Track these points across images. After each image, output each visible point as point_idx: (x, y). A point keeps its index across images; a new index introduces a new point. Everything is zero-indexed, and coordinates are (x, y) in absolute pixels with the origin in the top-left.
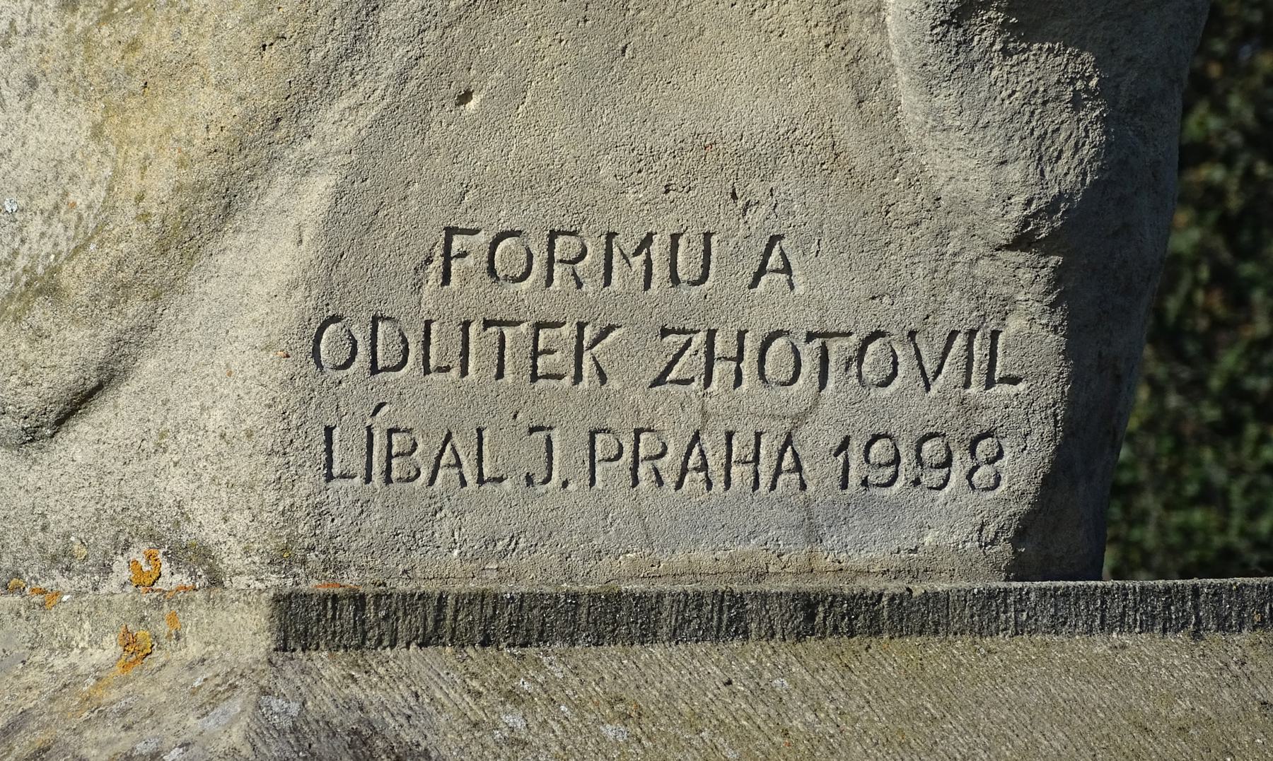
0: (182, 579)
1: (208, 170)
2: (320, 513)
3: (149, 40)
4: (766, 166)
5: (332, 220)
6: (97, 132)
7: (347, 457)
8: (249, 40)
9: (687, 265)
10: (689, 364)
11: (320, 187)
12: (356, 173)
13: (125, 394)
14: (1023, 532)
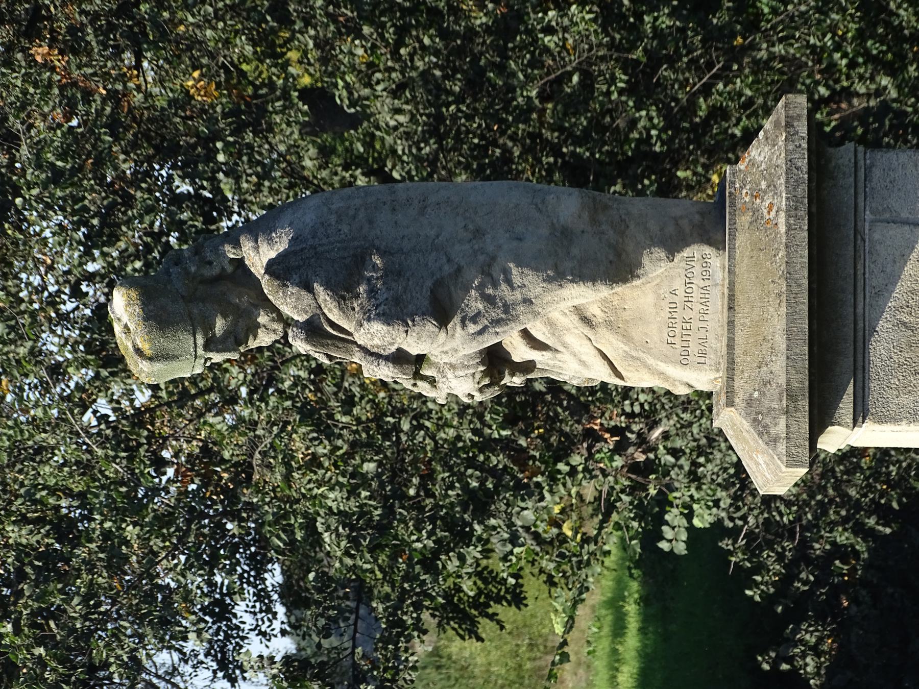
1: (656, 377)
2: (711, 365)
4: (659, 295)
5: (665, 362)
7: (702, 360)
9: (674, 306)
10: (689, 304)
11: (659, 363)
12: (658, 359)
14: (718, 249)
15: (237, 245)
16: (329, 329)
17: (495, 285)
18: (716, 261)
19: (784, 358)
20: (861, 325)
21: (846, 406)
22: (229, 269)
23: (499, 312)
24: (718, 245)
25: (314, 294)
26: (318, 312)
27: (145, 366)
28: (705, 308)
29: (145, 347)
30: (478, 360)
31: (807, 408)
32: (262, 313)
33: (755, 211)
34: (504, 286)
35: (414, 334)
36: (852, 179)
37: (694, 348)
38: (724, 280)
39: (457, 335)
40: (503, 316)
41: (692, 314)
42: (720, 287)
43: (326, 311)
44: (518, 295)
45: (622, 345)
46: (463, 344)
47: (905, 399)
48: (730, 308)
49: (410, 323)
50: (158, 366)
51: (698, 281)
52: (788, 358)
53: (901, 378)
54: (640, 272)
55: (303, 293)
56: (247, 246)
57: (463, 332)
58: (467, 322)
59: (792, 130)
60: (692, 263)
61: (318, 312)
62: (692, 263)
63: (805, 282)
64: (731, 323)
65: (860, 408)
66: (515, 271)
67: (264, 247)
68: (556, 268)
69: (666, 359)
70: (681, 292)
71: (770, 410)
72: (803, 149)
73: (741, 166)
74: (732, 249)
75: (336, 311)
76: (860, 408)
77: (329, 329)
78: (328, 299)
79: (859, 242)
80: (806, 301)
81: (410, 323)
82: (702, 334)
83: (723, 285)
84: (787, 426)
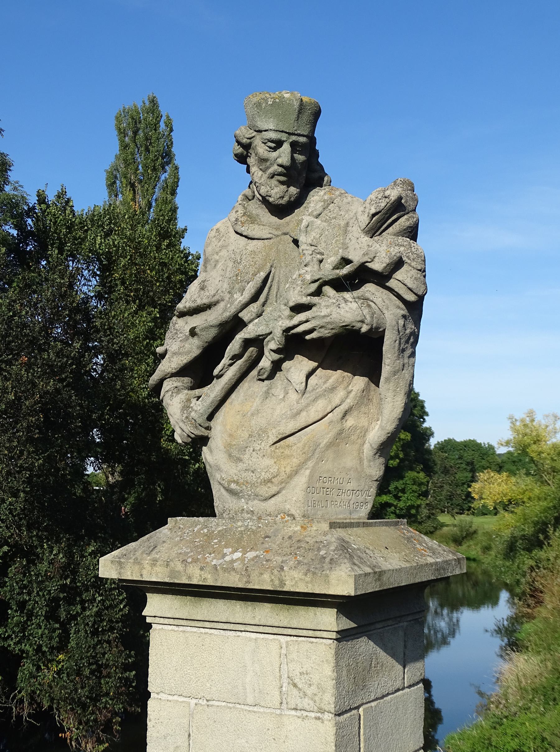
0: (289, 518)
1: (295, 469)
3: (286, 452)
6: (275, 463)
8: (301, 453)
10: (341, 493)
11: (308, 472)
12: (312, 470)
13: (280, 495)
18: (364, 511)
21: (347, 624)
26: (407, 211)
31: (376, 590)
32: (298, 190)
35: (419, 275)
38: (353, 519)
39: (398, 311)
42: (349, 517)
43: (406, 217)
45: (324, 443)
46: (393, 314)
47: (345, 673)
51: (354, 499)
52: (393, 570)
54: (377, 456)
69: (311, 476)
70: (350, 486)
74: (370, 525)
75: (408, 224)
79: (399, 619)
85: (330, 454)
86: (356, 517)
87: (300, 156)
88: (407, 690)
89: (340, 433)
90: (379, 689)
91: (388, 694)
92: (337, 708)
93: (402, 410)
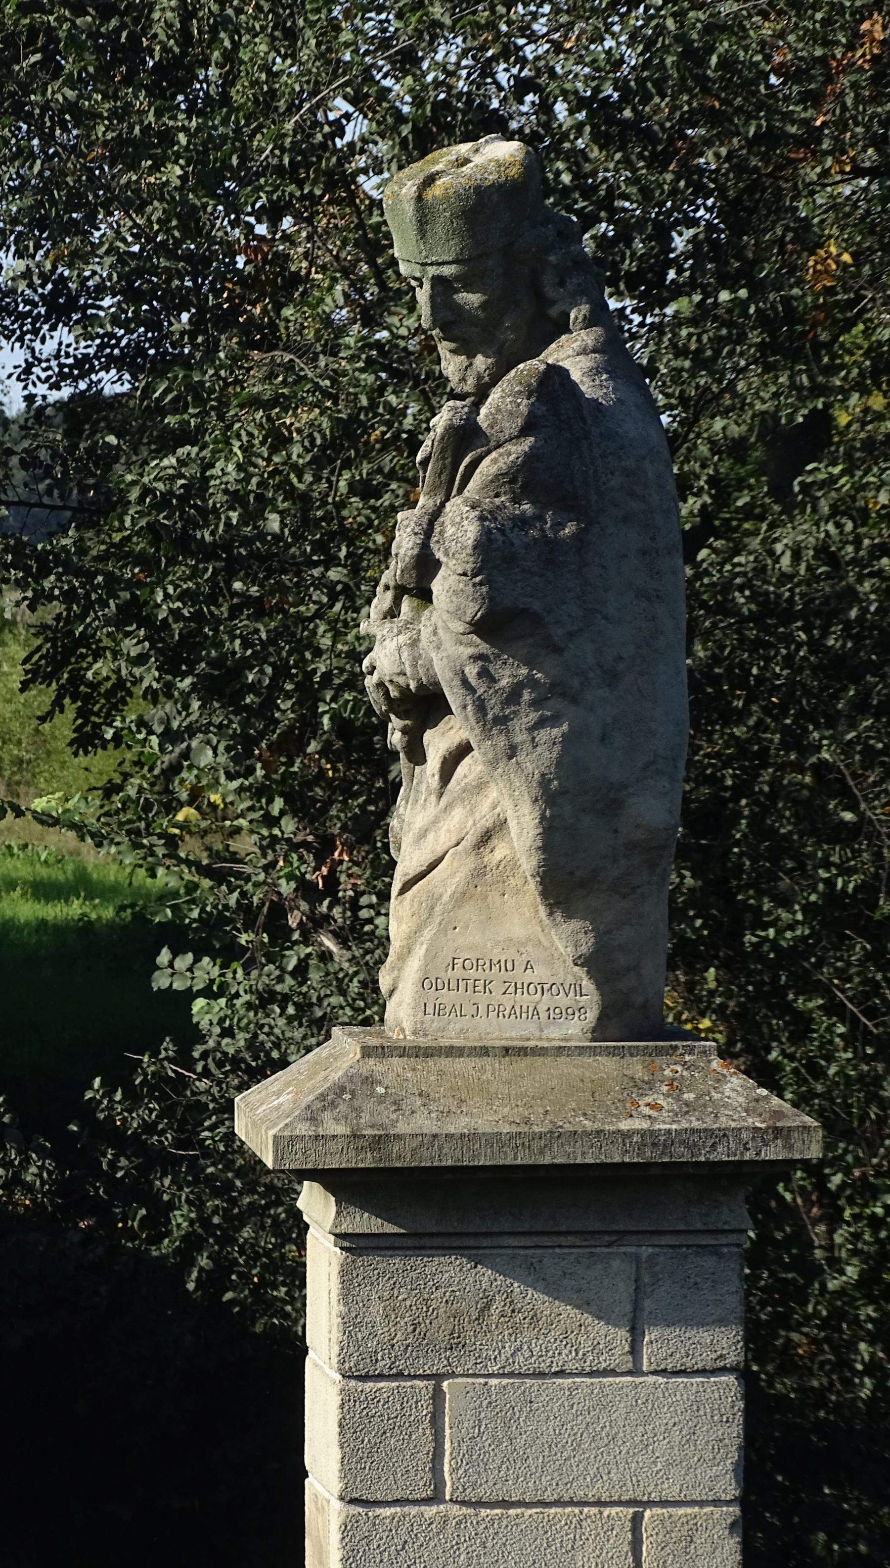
2: (422, 1023)
4: (524, 944)
5: (426, 956)
7: (430, 1010)
9: (509, 967)
10: (512, 989)
11: (425, 947)
14: (594, 1031)
15: (589, 323)
16: (467, 460)
17: (535, 704)
19: (435, 1130)
20: (486, 1242)
22: (554, 312)
23: (497, 710)
24: (600, 1031)
25: (517, 437)
26: (492, 444)
27: (409, 189)
28: (507, 1013)
29: (437, 190)
30: (424, 680)
33: (650, 1085)
34: (534, 716)
36: (699, 1226)
37: (446, 997)
39: (461, 649)
40: (490, 716)
41: (497, 995)
42: (537, 1034)
43: (494, 455)
44: (521, 737)
46: (448, 657)
47: (376, 1310)
48: (507, 1050)
49: (478, 579)
50: (409, 209)
52: (435, 1136)
53: (408, 1303)
54: (558, 916)
55: (520, 421)
56: (586, 337)
57: (465, 657)
58: (480, 663)
59: (771, 1137)
60: (572, 994)
61: (492, 444)
62: (572, 994)
63: (547, 1160)
64: (484, 1051)
65: (362, 1243)
66: (556, 732)
67: (586, 362)
68: (562, 792)
69: (430, 957)
70: (529, 977)
71: (358, 1111)
72: (742, 1154)
73: (716, 1063)
74: (594, 1052)
75: (494, 470)
76: (362, 1243)
77: (467, 460)
78: (512, 458)
79: (607, 1238)
80: (519, 1162)
81: (478, 579)
82: (468, 1009)
83: (540, 1039)
84: (334, 1137)
85: (469, 912)
86: (556, 1035)
87: (470, 295)
88: (651, 1379)
89: (480, 873)
90: (520, 1358)
91: (561, 1373)
92: (347, 1365)
93: (540, 830)
